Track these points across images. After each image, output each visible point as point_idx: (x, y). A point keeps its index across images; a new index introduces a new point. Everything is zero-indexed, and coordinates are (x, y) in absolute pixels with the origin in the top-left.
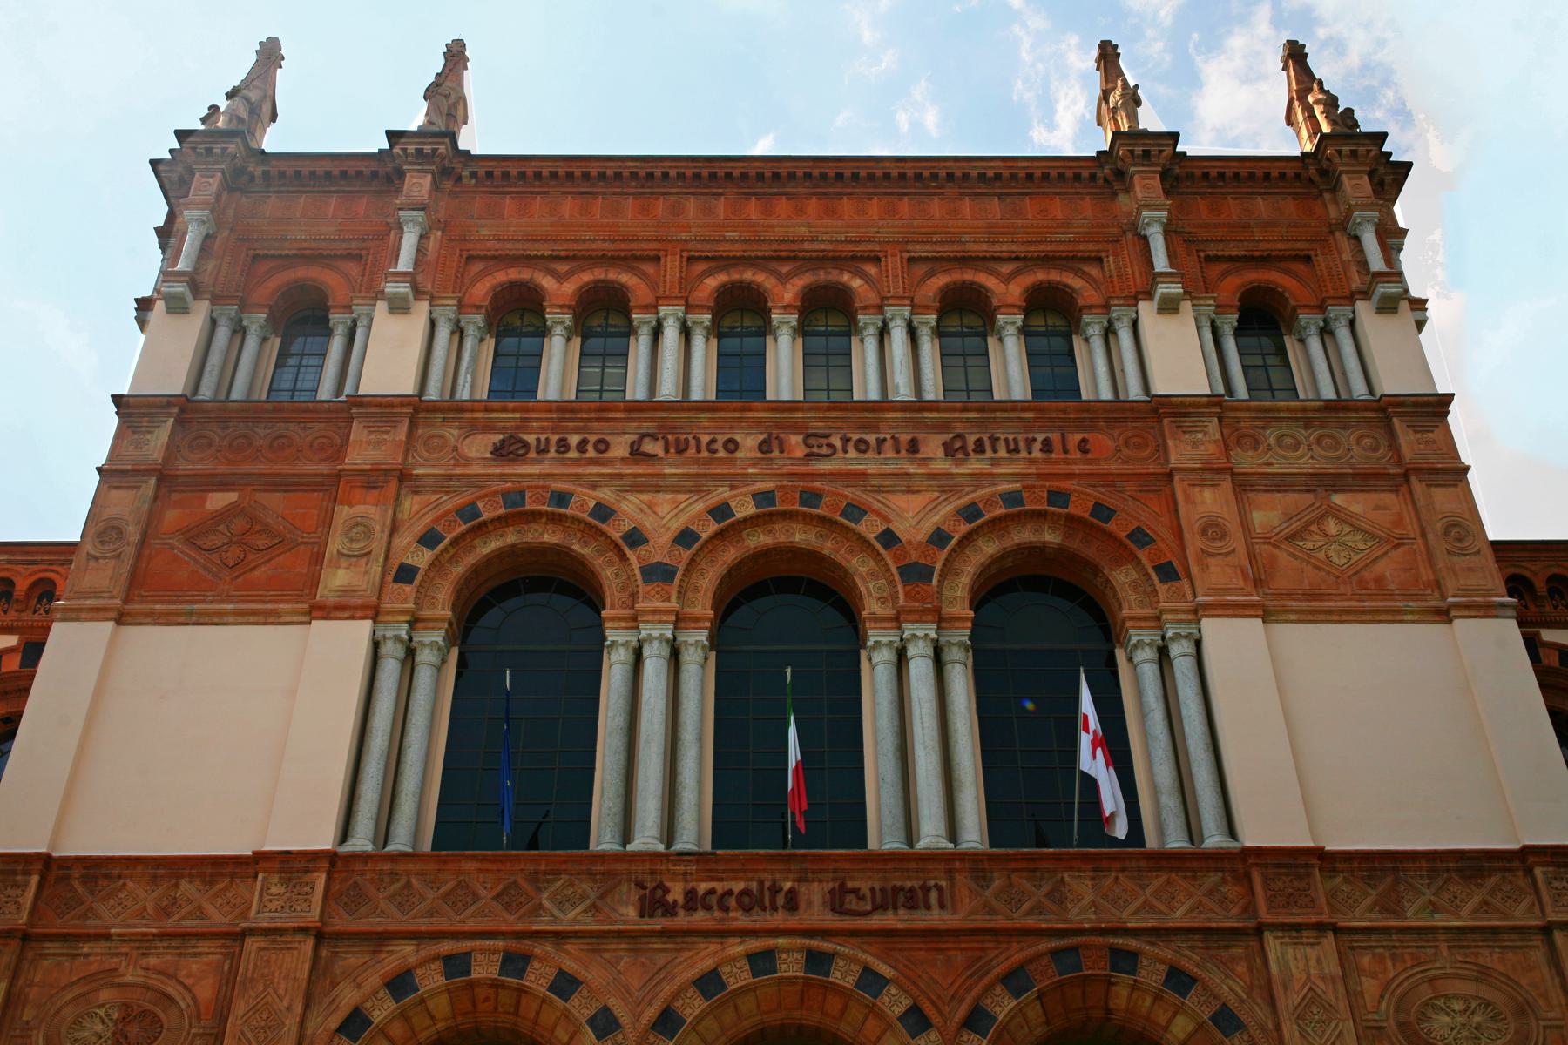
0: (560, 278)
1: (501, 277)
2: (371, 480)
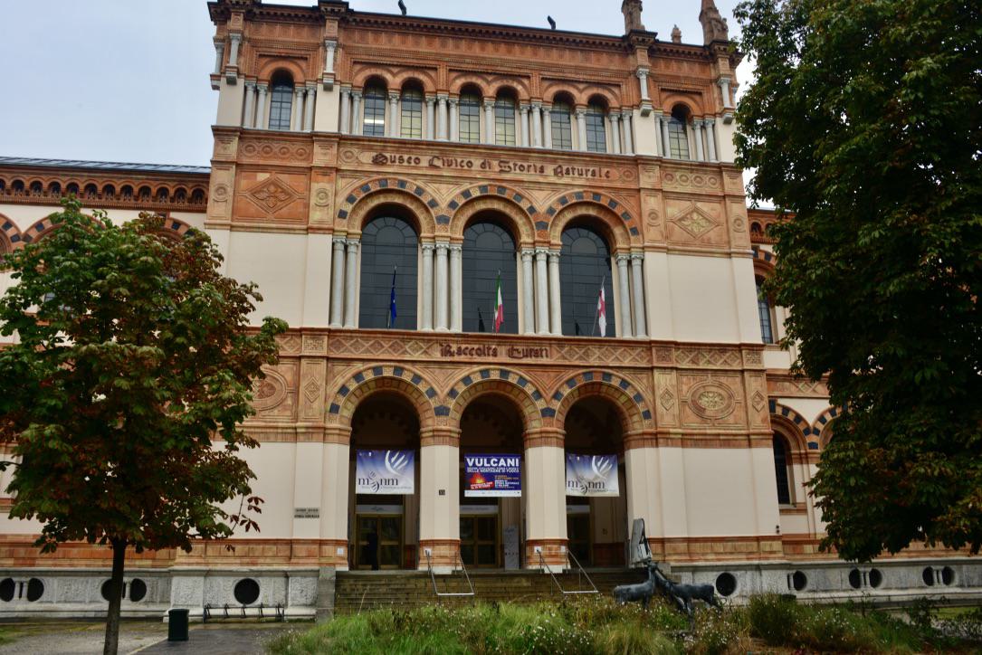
0: (394, 75)
2: (327, 171)
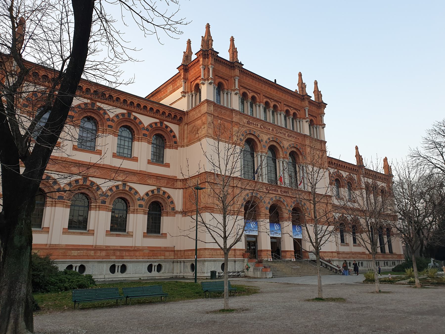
2: (237, 124)
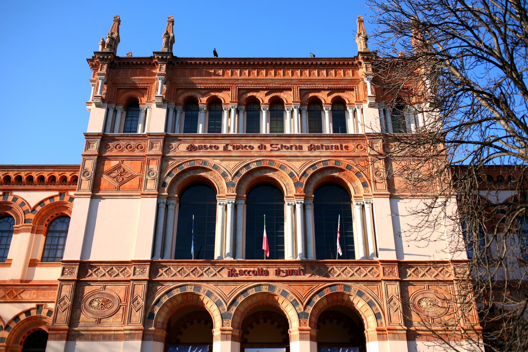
1: (187, 94)
